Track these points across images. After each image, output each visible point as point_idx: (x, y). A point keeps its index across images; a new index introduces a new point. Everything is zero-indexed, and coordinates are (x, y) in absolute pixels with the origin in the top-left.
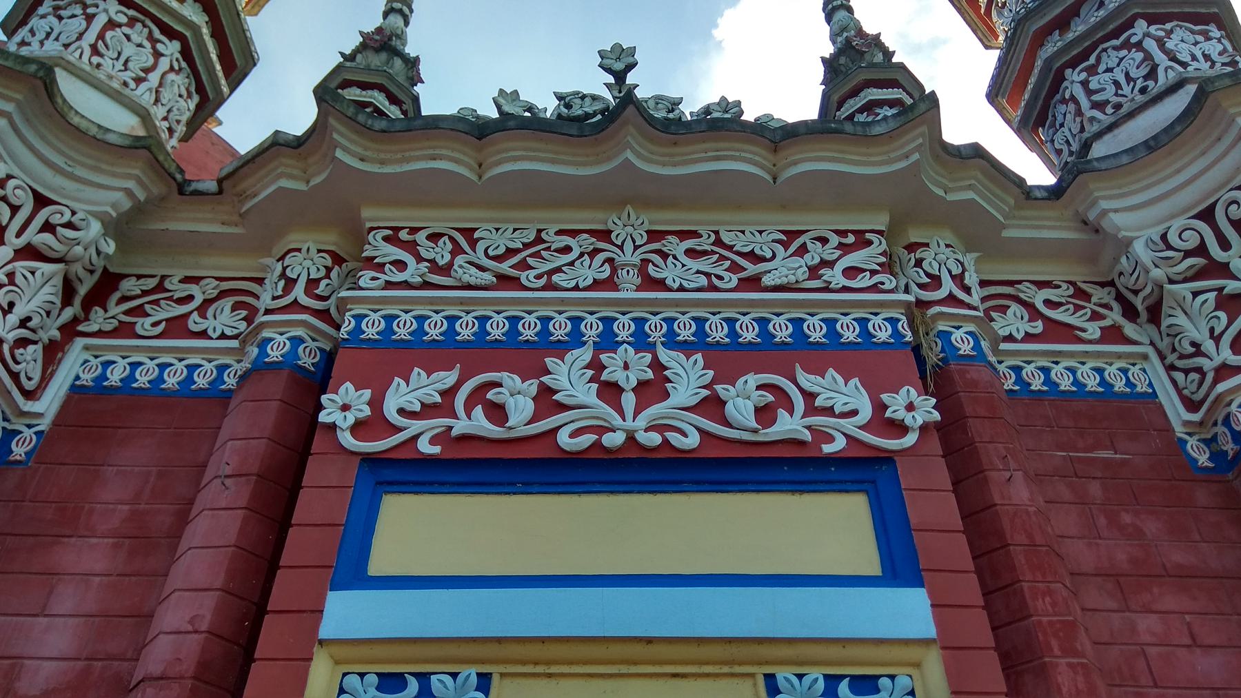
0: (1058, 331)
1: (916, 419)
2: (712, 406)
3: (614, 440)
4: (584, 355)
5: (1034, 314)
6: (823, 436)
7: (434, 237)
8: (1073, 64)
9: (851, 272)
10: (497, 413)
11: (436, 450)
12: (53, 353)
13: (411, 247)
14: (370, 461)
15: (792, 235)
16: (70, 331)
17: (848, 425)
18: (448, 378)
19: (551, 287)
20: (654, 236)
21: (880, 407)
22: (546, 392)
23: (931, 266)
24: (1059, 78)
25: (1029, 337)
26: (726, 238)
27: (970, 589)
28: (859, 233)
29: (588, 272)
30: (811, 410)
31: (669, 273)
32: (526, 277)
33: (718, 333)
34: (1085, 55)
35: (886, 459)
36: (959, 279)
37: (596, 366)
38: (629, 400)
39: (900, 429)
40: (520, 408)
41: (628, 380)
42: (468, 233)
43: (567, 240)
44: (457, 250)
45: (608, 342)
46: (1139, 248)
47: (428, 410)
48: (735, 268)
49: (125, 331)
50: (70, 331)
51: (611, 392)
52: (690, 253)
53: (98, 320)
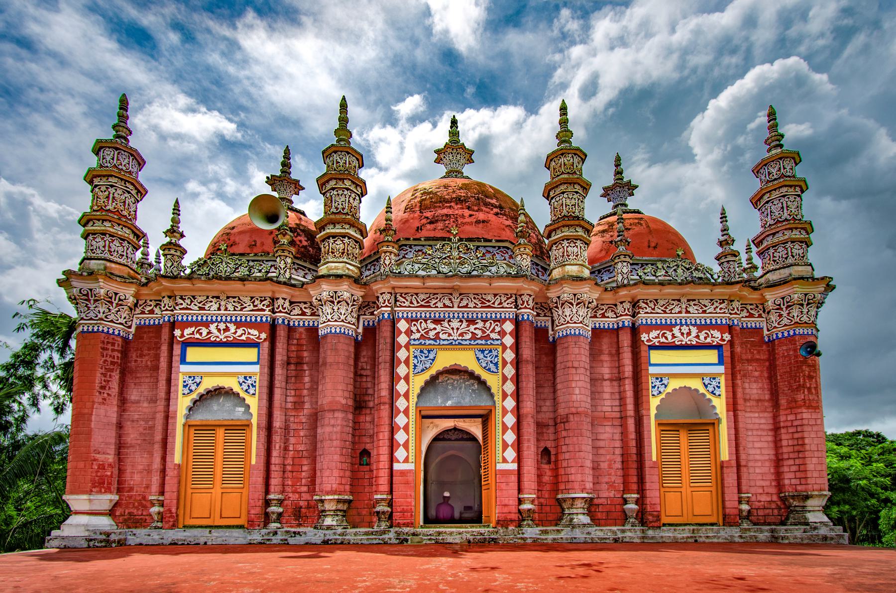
1: (727, 339)
2: (698, 337)
3: (683, 343)
4: (678, 327)
6: (713, 342)
7: (651, 302)
8: (773, 247)
9: (721, 309)
10: (666, 338)
11: (657, 344)
13: (647, 304)
14: (649, 346)
15: (712, 300)
17: (717, 340)
18: (658, 332)
19: (671, 313)
20: (688, 300)
21: (722, 337)
22: (673, 334)
23: (734, 306)
24: (769, 249)
26: (701, 301)
27: (729, 366)
28: (723, 300)
29: (677, 309)
30: (712, 337)
31: (690, 309)
32: (667, 310)
33: (698, 322)
34: (775, 246)
35: (721, 346)
36: (737, 308)
37: (680, 329)
38: (685, 336)
39: (724, 340)
40: (670, 337)
41: (685, 332)
42: (656, 300)
43: (673, 302)
44: (655, 305)
45: (682, 325)
46: (769, 302)
47: (656, 338)
48: (702, 308)
49: (595, 316)
51: (682, 334)
52: (694, 305)
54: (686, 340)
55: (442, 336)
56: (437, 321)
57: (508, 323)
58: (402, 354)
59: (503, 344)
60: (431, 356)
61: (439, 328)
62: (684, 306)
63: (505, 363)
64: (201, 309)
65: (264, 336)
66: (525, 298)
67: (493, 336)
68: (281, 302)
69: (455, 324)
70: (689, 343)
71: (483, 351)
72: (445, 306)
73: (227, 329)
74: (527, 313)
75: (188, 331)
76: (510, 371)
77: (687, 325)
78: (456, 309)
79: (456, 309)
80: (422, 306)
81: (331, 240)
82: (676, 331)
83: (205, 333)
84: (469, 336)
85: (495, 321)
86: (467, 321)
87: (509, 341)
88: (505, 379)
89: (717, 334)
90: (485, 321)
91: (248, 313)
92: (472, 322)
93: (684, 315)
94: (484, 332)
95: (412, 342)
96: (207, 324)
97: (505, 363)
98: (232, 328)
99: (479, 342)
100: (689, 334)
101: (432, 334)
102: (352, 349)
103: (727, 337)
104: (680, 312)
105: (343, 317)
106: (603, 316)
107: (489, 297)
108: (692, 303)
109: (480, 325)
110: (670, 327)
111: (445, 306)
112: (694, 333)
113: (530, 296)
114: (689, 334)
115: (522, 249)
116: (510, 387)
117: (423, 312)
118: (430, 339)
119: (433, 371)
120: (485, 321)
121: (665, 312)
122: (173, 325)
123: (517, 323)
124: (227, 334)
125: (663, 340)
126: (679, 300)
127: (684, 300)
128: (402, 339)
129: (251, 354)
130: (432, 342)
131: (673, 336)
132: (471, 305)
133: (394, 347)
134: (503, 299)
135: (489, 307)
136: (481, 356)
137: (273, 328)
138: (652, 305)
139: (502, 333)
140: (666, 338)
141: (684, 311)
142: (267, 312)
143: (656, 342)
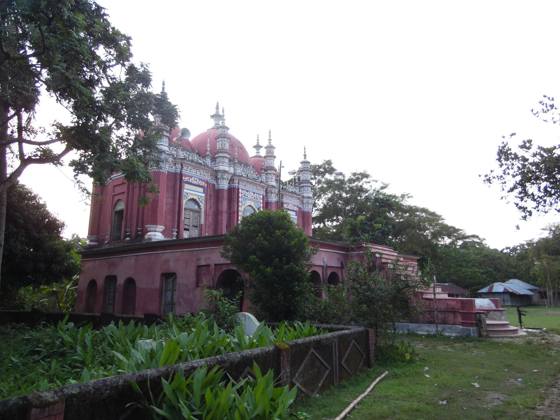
56: (247, 191)
58: (240, 199)
69: (251, 193)
73: (196, 180)
75: (186, 178)
81: (225, 158)
91: (202, 177)
92: (254, 193)
98: (198, 180)
107: (258, 187)
109: (256, 195)
117: (245, 188)
128: (240, 195)
129: (201, 190)
133: (238, 197)
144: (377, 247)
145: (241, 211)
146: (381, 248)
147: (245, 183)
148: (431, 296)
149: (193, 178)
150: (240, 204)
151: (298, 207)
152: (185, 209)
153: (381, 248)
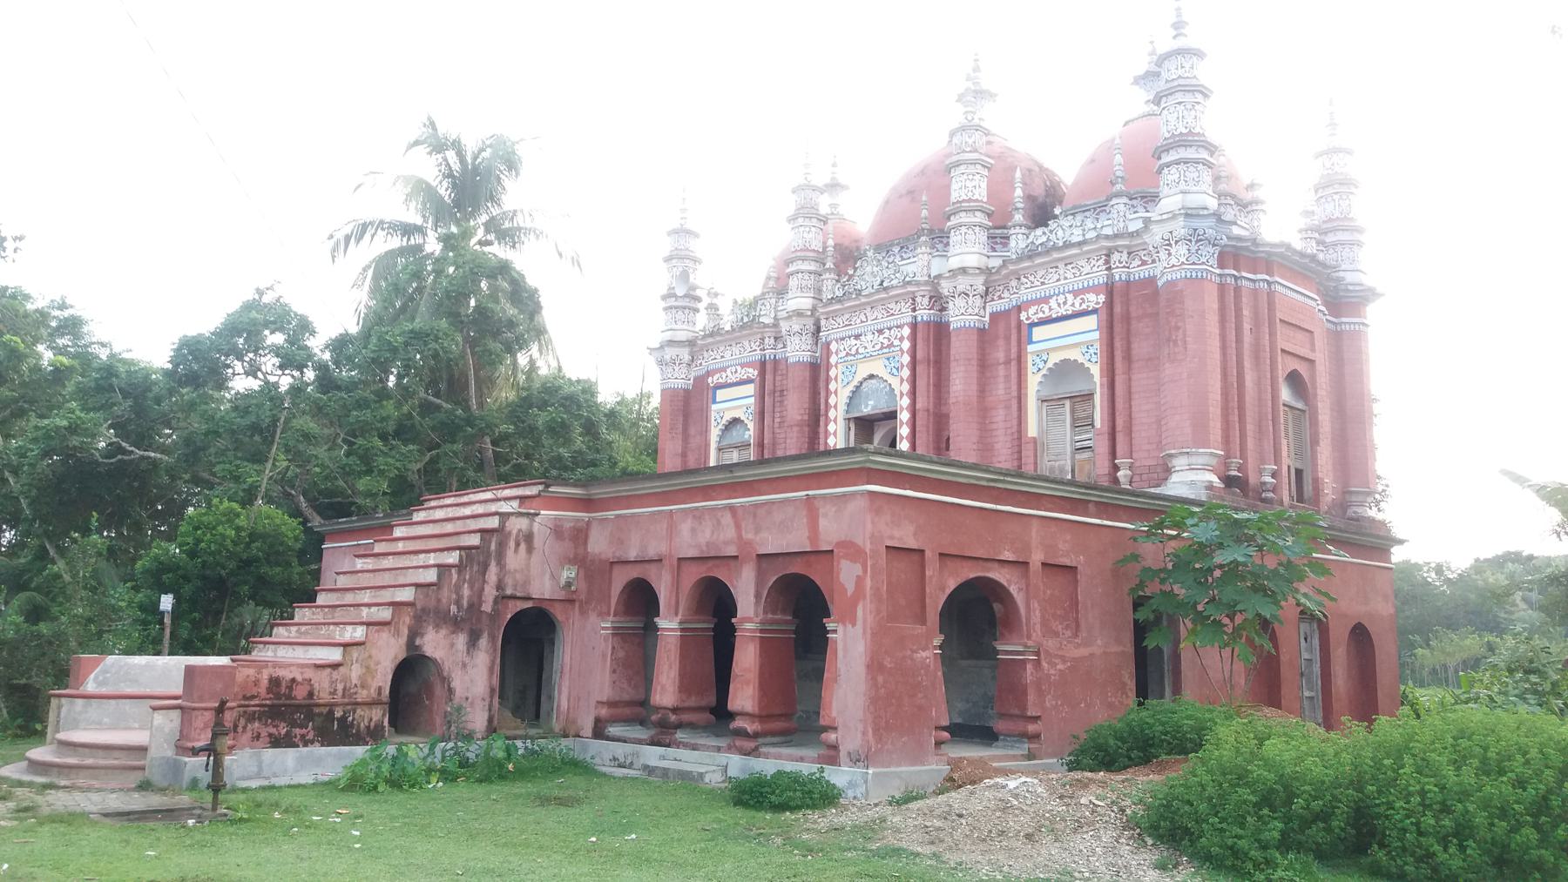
0: (1144, 263)
1: (1101, 301)
2: (1073, 305)
4: (1055, 298)
5: (1141, 259)
10: (1044, 312)
12: (984, 308)
13: (1027, 278)
16: (985, 303)
25: (1138, 266)
29: (1056, 277)
31: (1068, 275)
32: (1046, 281)
45: (1058, 295)
49: (993, 300)
50: (985, 303)
51: (1059, 305)
53: (989, 299)
54: (1063, 311)
55: (860, 351)
56: (857, 337)
57: (906, 328)
59: (901, 350)
60: (853, 371)
61: (858, 342)
62: (1061, 272)
63: (902, 366)
64: (722, 357)
65: (756, 373)
66: (919, 299)
67: (896, 342)
68: (767, 340)
69: (870, 337)
70: (1064, 313)
71: (888, 359)
72: (862, 322)
73: (736, 372)
74: (924, 314)
75: (715, 377)
76: (906, 373)
77: (1063, 294)
78: (869, 322)
79: (869, 322)
80: (847, 325)
82: (1053, 303)
83: (724, 376)
84: (878, 347)
85: (897, 327)
86: (878, 331)
87: (906, 345)
88: (902, 380)
89: (1092, 297)
90: (890, 329)
92: (880, 332)
93: (1062, 282)
94: (889, 340)
95: (840, 361)
96: (724, 369)
97: (902, 366)
98: (739, 368)
99: (885, 351)
100: (1065, 303)
101: (854, 349)
102: (807, 374)
103: (1102, 298)
104: (1058, 280)
105: (797, 348)
106: (1000, 298)
108: (1069, 267)
109: (886, 335)
110: (1046, 300)
111: (862, 322)
112: (1069, 302)
113: (923, 296)
114: (1065, 303)
115: (923, 248)
116: (906, 387)
118: (851, 355)
119: (855, 383)
120: (890, 329)
121: (1043, 283)
122: (709, 374)
123: (914, 326)
124: (737, 375)
125: (1041, 315)
126: (1057, 267)
127: (1061, 265)
130: (852, 358)
131: (1050, 309)
132: (880, 316)
134: (903, 304)
135: (893, 315)
136: (887, 363)
137: (762, 365)
138: (1032, 278)
139: (901, 339)
140: (1044, 312)
141: (1062, 277)
142: (758, 352)
143: (1035, 319)
144: (473, 497)
145: (835, 407)
146: (488, 495)
147: (847, 316)
148: (275, 651)
149: (728, 370)
150: (832, 386)
151: (1094, 289)
152: (720, 449)
153: (488, 495)
